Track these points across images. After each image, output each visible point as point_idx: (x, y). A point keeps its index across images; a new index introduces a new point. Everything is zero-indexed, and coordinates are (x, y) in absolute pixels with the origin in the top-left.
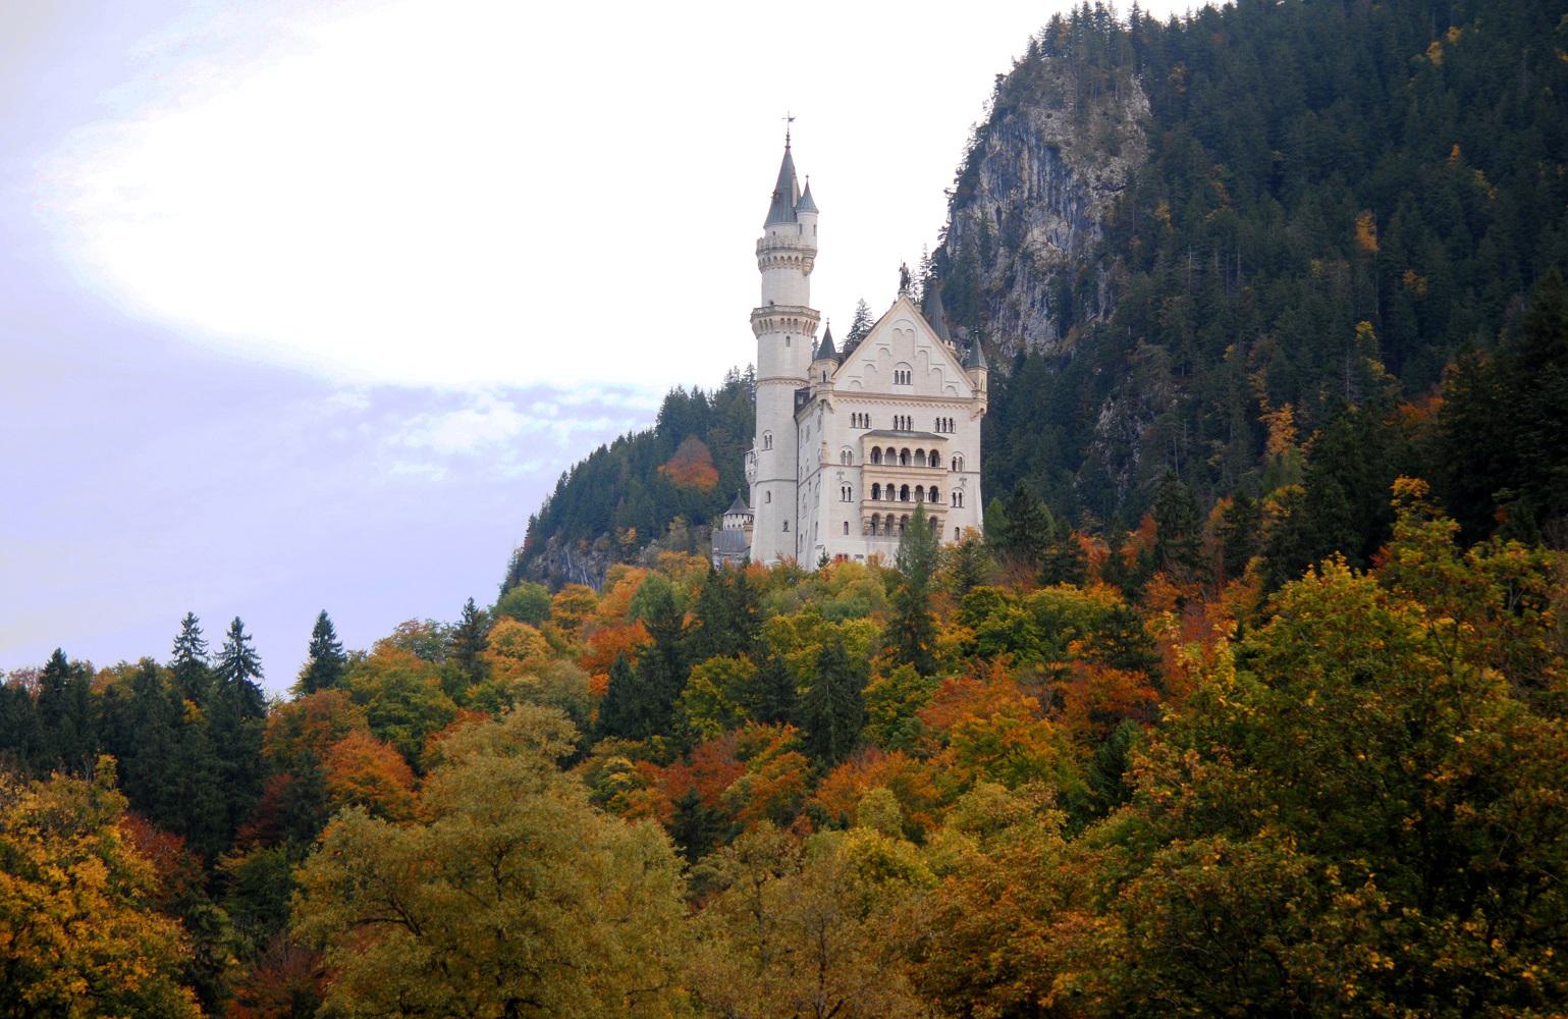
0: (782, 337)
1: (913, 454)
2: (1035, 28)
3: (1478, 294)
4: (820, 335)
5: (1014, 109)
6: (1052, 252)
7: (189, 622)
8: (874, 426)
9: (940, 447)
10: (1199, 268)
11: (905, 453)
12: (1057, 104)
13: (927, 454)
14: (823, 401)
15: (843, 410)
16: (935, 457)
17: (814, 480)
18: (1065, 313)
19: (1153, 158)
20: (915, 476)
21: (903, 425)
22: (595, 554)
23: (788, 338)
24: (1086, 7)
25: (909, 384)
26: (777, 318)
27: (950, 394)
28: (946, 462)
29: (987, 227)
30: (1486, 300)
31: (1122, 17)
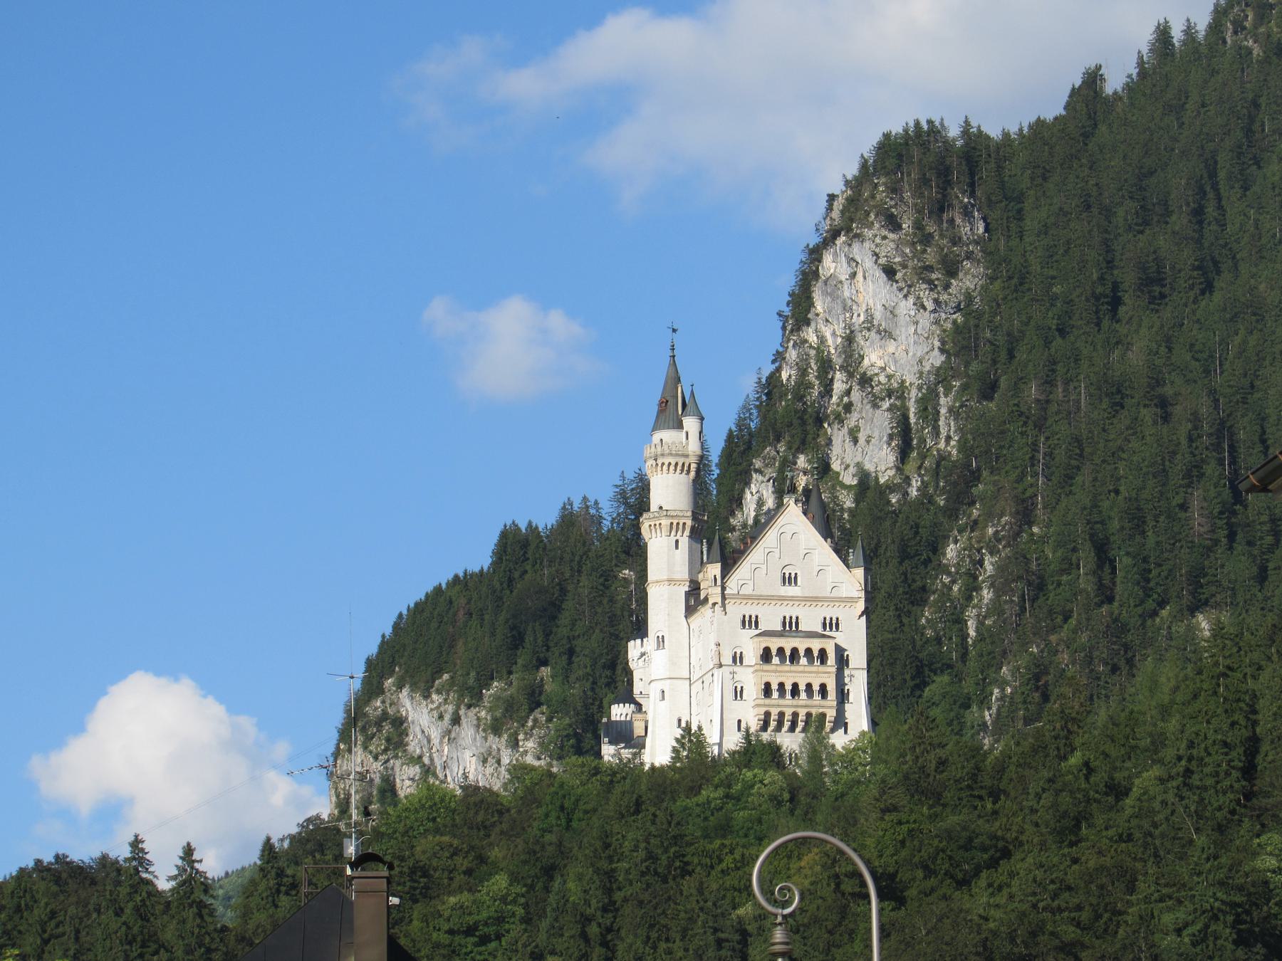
1: (802, 653)
2: (867, 144)
5: (849, 230)
6: (889, 377)
8: (763, 627)
11: (795, 651)
17: (708, 678)
18: (904, 440)
21: (790, 627)
23: (677, 542)
24: (917, 123)
31: (954, 131)
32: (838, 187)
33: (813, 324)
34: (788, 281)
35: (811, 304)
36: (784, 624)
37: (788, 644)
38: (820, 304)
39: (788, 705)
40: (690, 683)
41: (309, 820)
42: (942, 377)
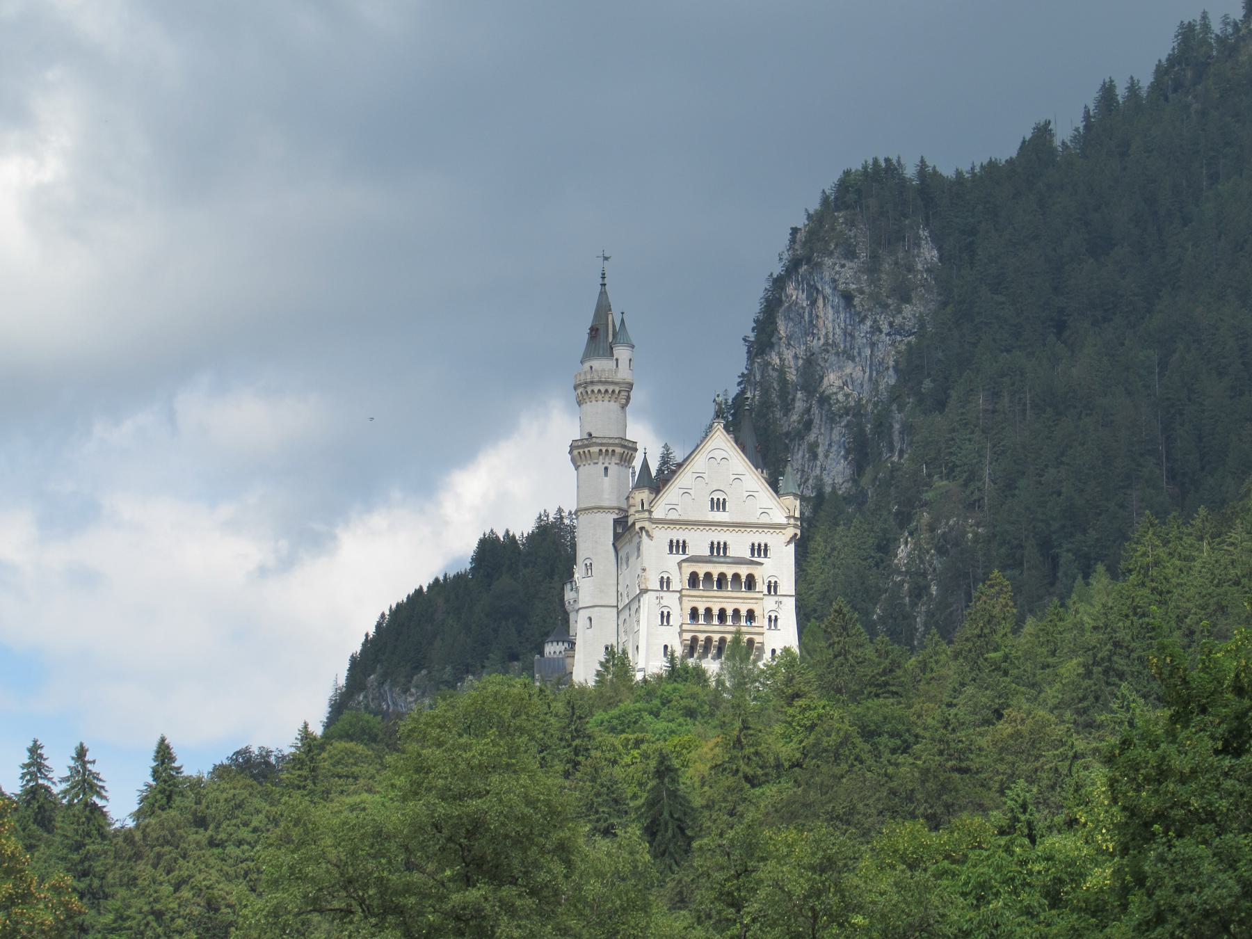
0: (601, 467)
2: (828, 181)
4: (637, 464)
5: (809, 260)
6: (847, 396)
7: (35, 750)
8: (691, 552)
9: (757, 572)
10: (990, 407)
11: (722, 577)
12: (850, 254)
13: (743, 579)
14: (642, 529)
15: (663, 536)
16: (751, 582)
18: (861, 453)
19: (945, 304)
20: (730, 600)
21: (719, 550)
22: (413, 690)
23: (606, 469)
24: (876, 161)
25: (724, 509)
26: (595, 449)
27: (764, 520)
28: (761, 587)
29: (785, 373)
31: (910, 171)
34: (754, 308)
35: (776, 330)
38: (783, 328)
39: (716, 632)
40: (629, 624)
41: (237, 753)
42: (895, 396)
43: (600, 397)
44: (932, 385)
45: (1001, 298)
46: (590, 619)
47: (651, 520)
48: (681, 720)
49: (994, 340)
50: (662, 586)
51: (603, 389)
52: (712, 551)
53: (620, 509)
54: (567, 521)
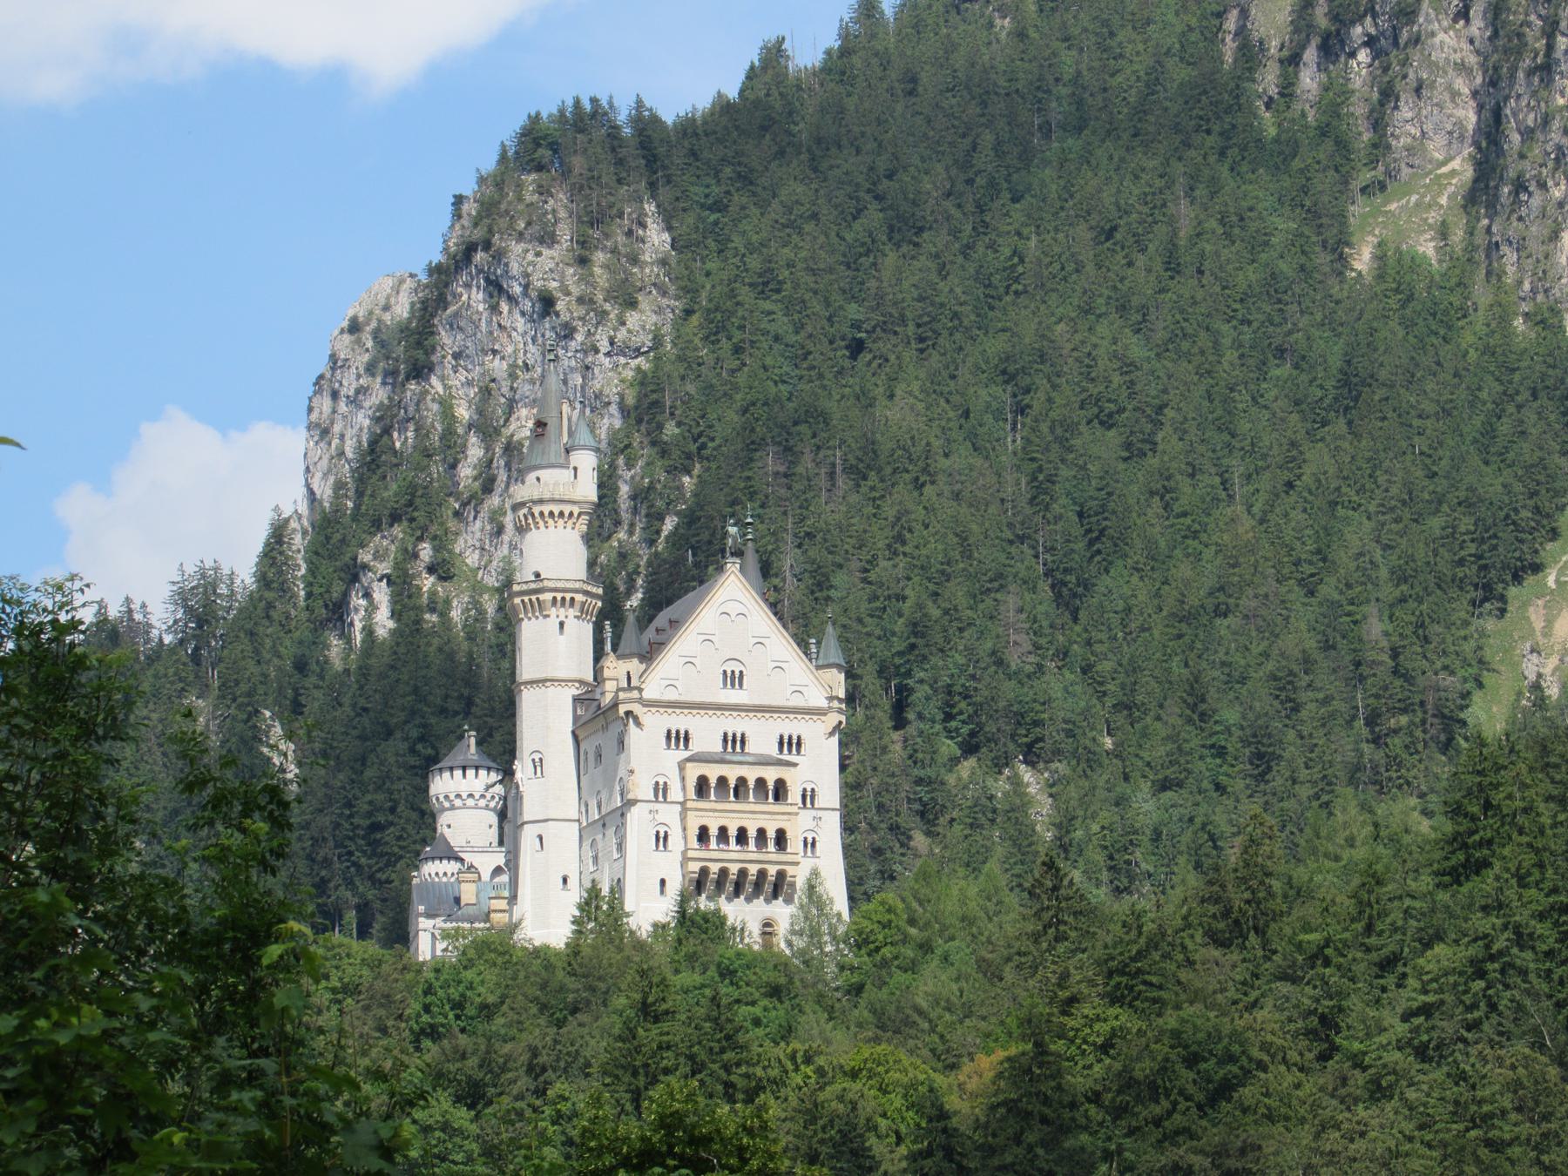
0: (553, 622)
2: (508, 128)
3: (1166, 507)
5: (487, 245)
8: (696, 746)
10: (782, 469)
11: (742, 781)
12: (547, 238)
14: (628, 713)
15: (655, 724)
16: (780, 791)
19: (688, 312)
23: (562, 624)
24: (577, 102)
26: (548, 596)
27: (797, 701)
28: (794, 795)
29: (451, 407)
30: (1178, 516)
31: (622, 117)
32: (469, 188)
33: (438, 370)
36: (725, 740)
37: (732, 773)
38: (447, 340)
39: (732, 858)
43: (561, 522)
44: (677, 431)
45: (768, 306)
46: (541, 838)
47: (641, 701)
48: (765, 1002)
49: (765, 368)
50: (656, 795)
51: (556, 509)
52: (725, 748)
53: (581, 682)
54: (138, 617)
